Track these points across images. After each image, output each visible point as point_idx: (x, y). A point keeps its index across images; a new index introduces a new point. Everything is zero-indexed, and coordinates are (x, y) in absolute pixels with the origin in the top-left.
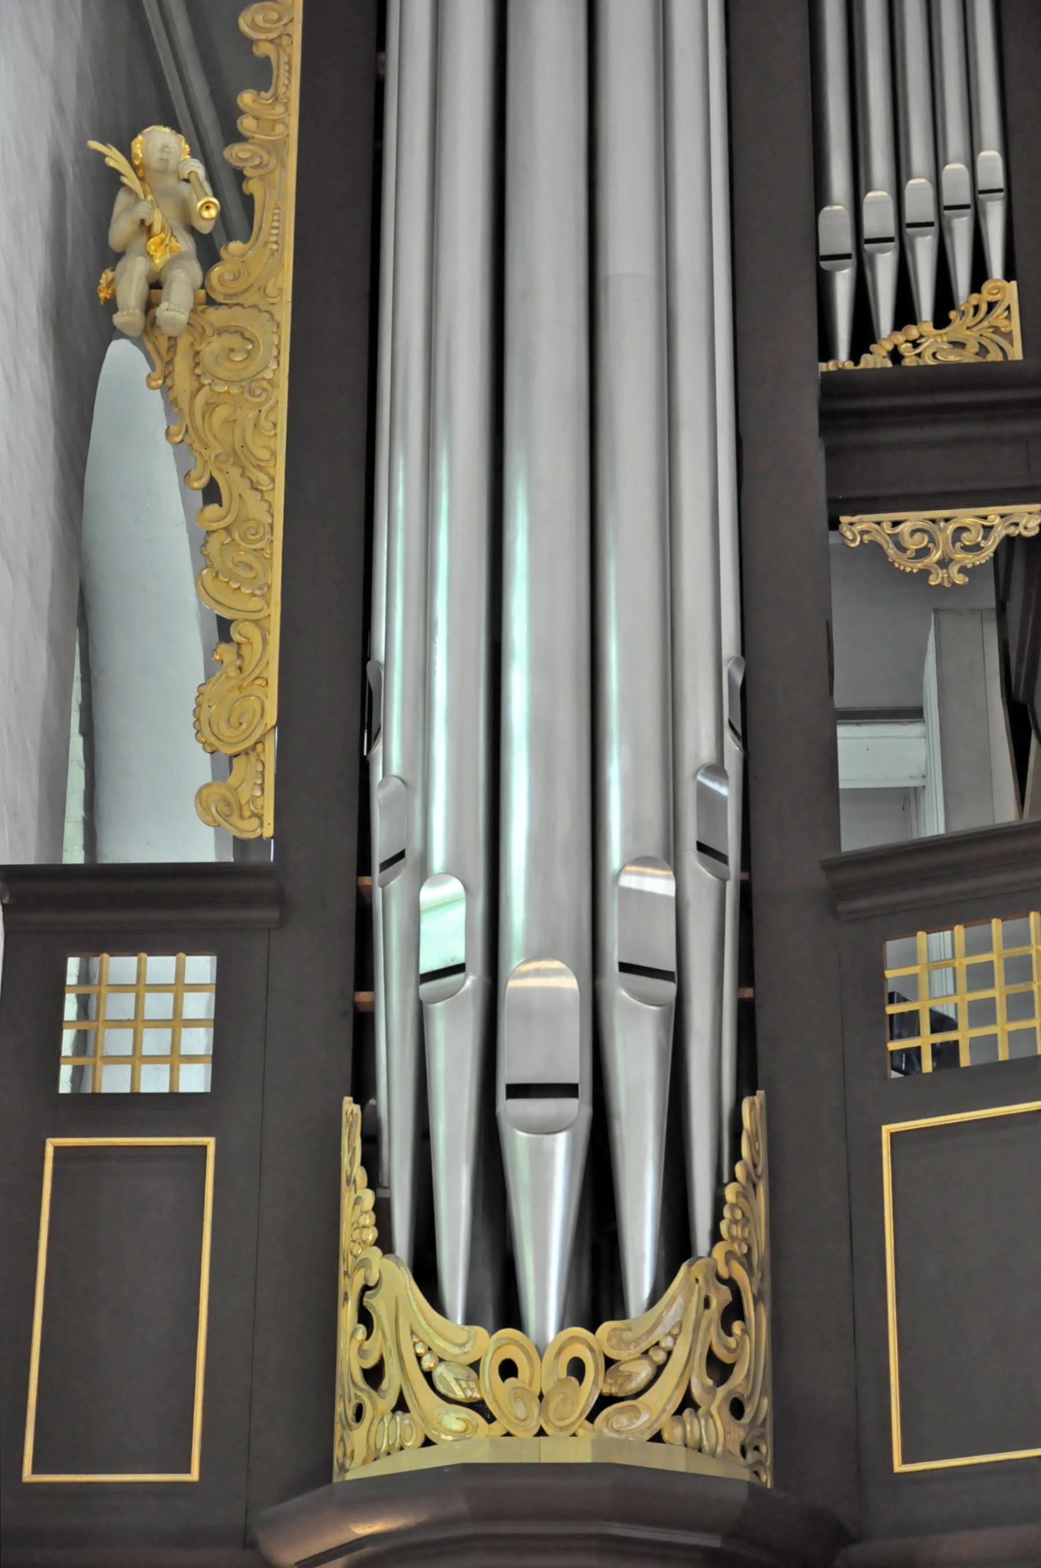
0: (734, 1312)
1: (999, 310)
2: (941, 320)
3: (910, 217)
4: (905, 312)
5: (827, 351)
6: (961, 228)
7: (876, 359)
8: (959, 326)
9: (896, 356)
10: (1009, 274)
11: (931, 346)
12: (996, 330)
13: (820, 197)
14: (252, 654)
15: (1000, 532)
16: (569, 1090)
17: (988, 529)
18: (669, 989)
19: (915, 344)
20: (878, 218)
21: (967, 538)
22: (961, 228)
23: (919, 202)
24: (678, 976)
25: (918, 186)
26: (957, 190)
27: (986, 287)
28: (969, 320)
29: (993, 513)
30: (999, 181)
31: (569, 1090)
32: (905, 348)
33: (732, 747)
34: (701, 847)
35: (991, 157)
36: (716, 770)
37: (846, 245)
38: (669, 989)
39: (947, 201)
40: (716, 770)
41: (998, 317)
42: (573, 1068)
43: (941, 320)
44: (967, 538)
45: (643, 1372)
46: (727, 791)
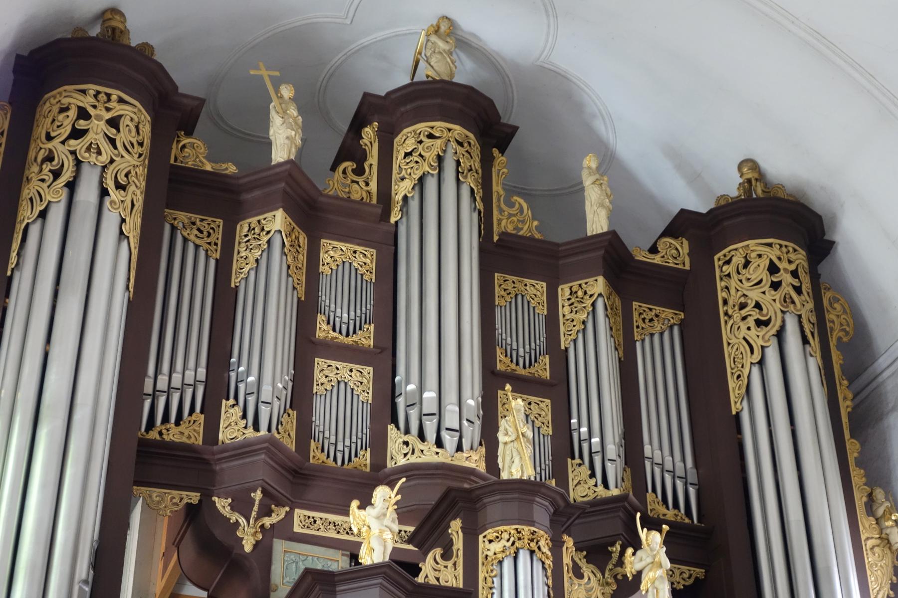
1: (197, 424)
2: (178, 423)
3: (173, 385)
4: (166, 419)
6: (189, 392)
8: (182, 428)
9: (161, 433)
10: (202, 412)
11: (173, 434)
12: (195, 430)
15: (185, 501)
17: (181, 499)
19: (168, 430)
20: (162, 384)
21: (174, 501)
22: (189, 392)
26: (189, 379)
27: (194, 415)
28: (187, 425)
29: (184, 493)
30: (204, 379)
32: (164, 431)
35: (202, 372)
37: (150, 391)
39: (186, 382)
41: (195, 427)
43: (178, 423)
44: (174, 501)
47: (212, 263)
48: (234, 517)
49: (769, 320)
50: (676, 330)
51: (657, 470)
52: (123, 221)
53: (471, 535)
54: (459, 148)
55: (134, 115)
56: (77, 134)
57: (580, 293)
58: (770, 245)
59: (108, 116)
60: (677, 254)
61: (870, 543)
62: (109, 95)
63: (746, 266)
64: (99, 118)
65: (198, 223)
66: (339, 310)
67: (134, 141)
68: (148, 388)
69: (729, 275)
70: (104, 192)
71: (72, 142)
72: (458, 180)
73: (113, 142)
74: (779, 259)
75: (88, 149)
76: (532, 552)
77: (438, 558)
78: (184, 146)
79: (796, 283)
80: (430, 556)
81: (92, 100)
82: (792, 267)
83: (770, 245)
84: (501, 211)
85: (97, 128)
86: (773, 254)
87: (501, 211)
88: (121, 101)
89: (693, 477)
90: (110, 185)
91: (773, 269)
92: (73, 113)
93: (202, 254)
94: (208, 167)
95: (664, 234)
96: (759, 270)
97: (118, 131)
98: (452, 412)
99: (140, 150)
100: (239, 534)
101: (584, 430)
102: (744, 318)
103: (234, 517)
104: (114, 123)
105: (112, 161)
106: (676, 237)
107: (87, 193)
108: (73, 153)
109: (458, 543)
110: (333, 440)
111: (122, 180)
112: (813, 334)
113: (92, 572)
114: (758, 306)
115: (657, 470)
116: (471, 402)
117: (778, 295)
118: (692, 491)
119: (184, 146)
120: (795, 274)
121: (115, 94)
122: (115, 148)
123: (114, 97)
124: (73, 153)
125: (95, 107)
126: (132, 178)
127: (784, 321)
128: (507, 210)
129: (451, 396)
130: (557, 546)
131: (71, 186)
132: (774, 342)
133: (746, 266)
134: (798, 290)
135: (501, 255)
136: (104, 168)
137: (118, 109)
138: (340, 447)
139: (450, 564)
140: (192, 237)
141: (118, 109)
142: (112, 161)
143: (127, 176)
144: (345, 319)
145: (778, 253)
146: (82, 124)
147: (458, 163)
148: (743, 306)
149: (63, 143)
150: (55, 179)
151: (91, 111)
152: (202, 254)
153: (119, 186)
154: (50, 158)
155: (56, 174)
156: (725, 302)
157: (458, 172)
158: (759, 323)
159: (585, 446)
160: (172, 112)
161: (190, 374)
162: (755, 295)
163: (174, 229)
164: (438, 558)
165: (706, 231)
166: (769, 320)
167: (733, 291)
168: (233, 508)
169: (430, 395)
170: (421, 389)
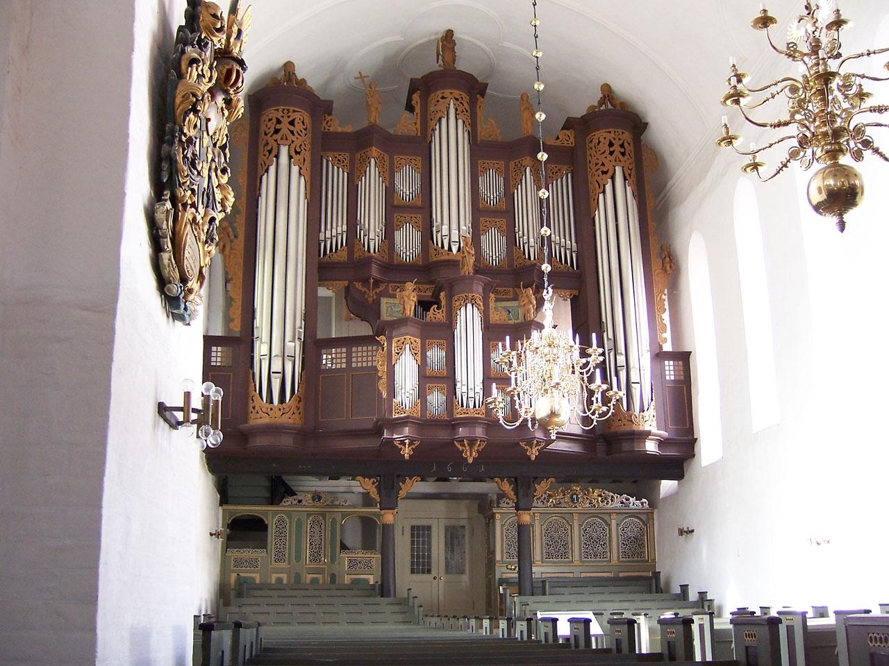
0: (300, 401)
5: (320, 256)
7: (327, 257)
13: (320, 231)
16: (280, 373)
18: (293, 358)
20: (328, 235)
23: (334, 234)
24: (294, 357)
25: (334, 231)
26: (339, 231)
31: (280, 373)
36: (301, 328)
40: (301, 328)
42: (280, 370)
45: (288, 410)
46: (302, 331)
47: (346, 174)
48: (364, 289)
49: (608, 171)
50: (569, 175)
51: (557, 247)
52: (301, 168)
53: (450, 298)
54: (456, 102)
55: (301, 116)
56: (277, 131)
57: (520, 165)
58: (610, 132)
60: (568, 139)
61: (657, 272)
63: (598, 144)
66: (404, 189)
68: (322, 237)
69: (591, 148)
71: (275, 135)
72: (456, 117)
73: (292, 132)
74: (614, 139)
75: (282, 139)
76: (473, 305)
77: (435, 309)
79: (622, 150)
80: (432, 308)
81: (282, 114)
82: (621, 142)
83: (610, 132)
84: (482, 128)
85: (285, 127)
86: (611, 136)
87: (482, 128)
88: (294, 111)
89: (574, 248)
91: (611, 144)
92: (274, 121)
93: (341, 170)
94: (340, 130)
95: (562, 129)
96: (604, 147)
97: (294, 126)
98: (454, 234)
100: (366, 296)
101: (521, 233)
102: (597, 171)
103: (364, 289)
104: (292, 123)
106: (568, 129)
108: (276, 141)
109: (443, 303)
110: (405, 251)
111: (298, 150)
112: (630, 175)
113: (303, 322)
114: (603, 164)
115: (557, 247)
116: (464, 228)
117: (609, 157)
118: (574, 255)
120: (622, 146)
121: (292, 108)
122: (293, 135)
123: (291, 111)
124: (276, 141)
125: (283, 117)
126: (303, 147)
127: (615, 169)
128: (485, 127)
129: (454, 226)
130: (486, 299)
132: (610, 181)
133: (598, 144)
134: (623, 154)
135: (483, 152)
138: (408, 254)
139: (440, 311)
142: (293, 142)
144: (408, 194)
145: (614, 136)
146: (278, 127)
147: (456, 110)
148: (597, 164)
149: (271, 136)
150: (270, 154)
151: (281, 119)
152: (341, 170)
153: (297, 153)
154: (267, 144)
155: (270, 152)
156: (590, 162)
157: (456, 114)
158: (604, 173)
159: (521, 239)
160: (318, 106)
161: (339, 228)
162: (602, 159)
164: (435, 309)
165: (582, 126)
166: (608, 171)
167: (593, 156)
168: (362, 286)
169: (445, 227)
170: (442, 224)
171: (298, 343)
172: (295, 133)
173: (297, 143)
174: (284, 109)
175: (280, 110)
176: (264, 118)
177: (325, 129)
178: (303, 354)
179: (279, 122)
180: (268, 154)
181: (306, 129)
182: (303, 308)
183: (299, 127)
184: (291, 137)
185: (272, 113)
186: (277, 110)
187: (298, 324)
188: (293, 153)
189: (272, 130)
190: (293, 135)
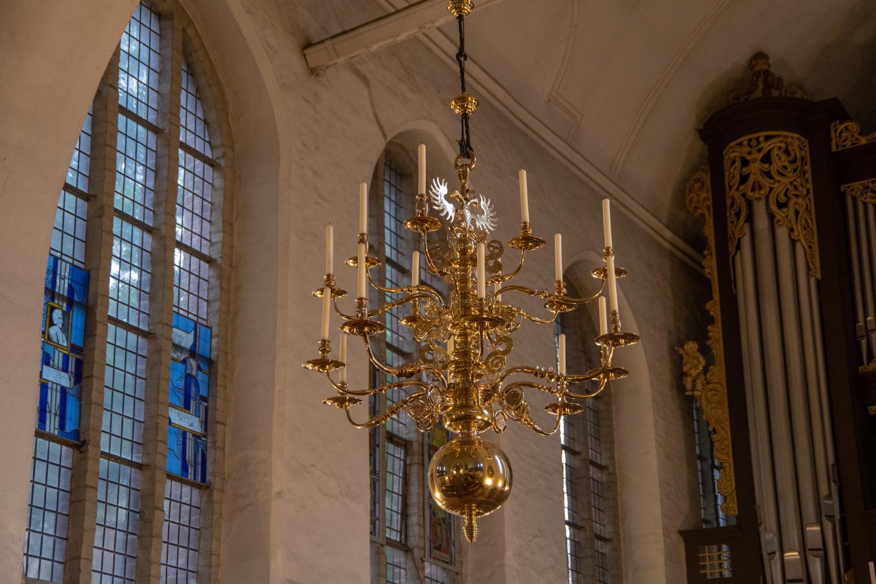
13: (855, 320)
14: (727, 469)
33: (834, 487)
34: (826, 516)
36: (829, 496)
38: (822, 553)
52: (792, 230)
56: (744, 179)
59: (760, 156)
62: (757, 139)
64: (754, 160)
65: (871, 185)
67: (786, 164)
70: (771, 216)
71: (742, 187)
73: (768, 174)
75: (753, 190)
78: (841, 132)
81: (746, 149)
85: (755, 168)
88: (767, 138)
90: (774, 208)
92: (738, 164)
94: (863, 141)
99: (794, 166)
104: (767, 159)
105: (771, 189)
107: (762, 223)
108: (744, 195)
111: (782, 199)
119: (841, 132)
121: (762, 135)
122: (771, 177)
123: (762, 139)
131: (750, 219)
136: (767, 197)
137: (766, 146)
140: (869, 200)
141: (766, 146)
142: (771, 189)
143: (786, 195)
149: (737, 189)
151: (749, 158)
153: (781, 206)
155: (738, 215)
163: (854, 199)
171: (828, 525)
172: (774, 174)
173: (779, 189)
174: (750, 140)
175: (745, 143)
176: (727, 164)
177: (837, 147)
178: (845, 538)
179: (745, 163)
180: (735, 219)
181: (794, 161)
182: (831, 461)
183: (779, 161)
184: (766, 183)
185: (733, 152)
186: (741, 144)
187: (824, 491)
188: (774, 208)
189: (737, 179)
190: (771, 177)
